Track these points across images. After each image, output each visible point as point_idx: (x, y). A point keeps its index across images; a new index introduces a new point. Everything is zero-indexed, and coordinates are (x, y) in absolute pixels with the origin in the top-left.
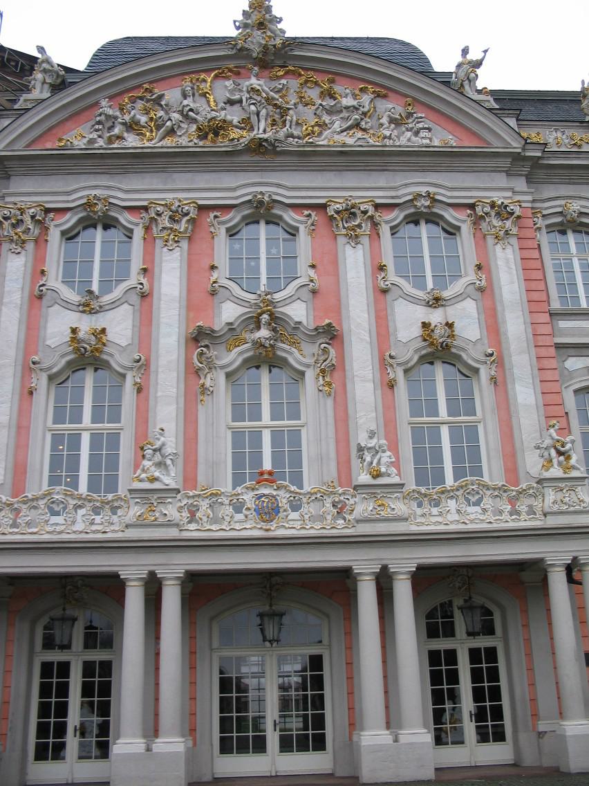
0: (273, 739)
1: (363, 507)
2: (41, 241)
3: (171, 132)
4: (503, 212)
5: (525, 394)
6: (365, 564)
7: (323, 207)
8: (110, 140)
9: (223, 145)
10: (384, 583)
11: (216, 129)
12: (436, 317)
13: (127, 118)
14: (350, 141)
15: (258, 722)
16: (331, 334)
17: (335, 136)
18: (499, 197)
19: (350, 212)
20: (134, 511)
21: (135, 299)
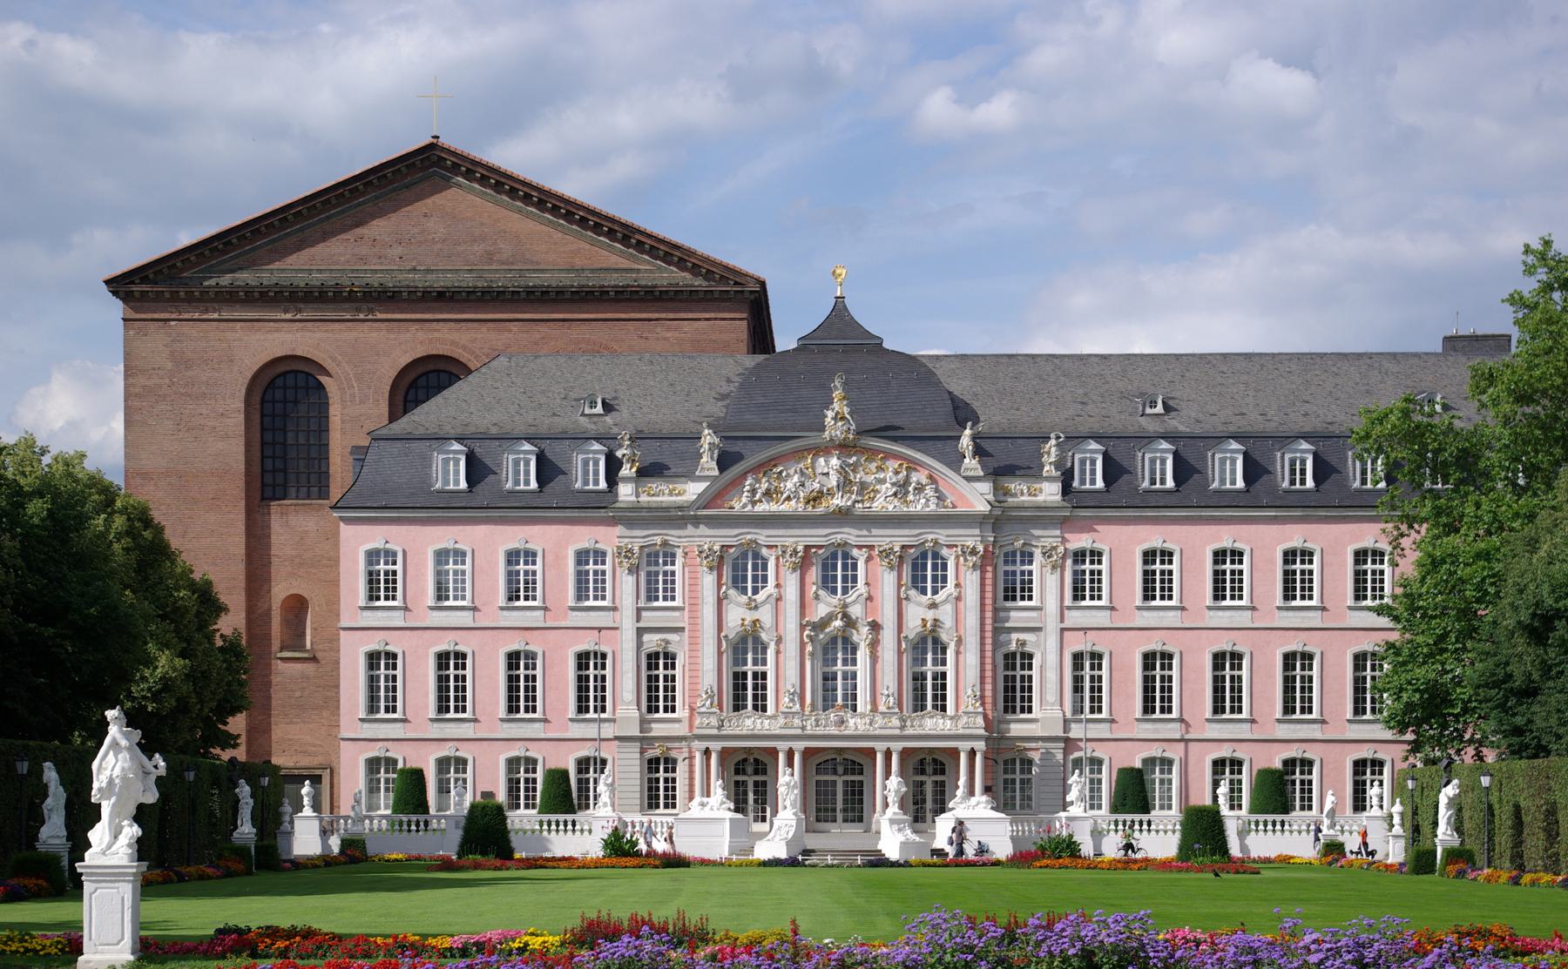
0: (840, 816)
1: (879, 720)
2: (719, 568)
3: (788, 499)
4: (974, 552)
5: (971, 658)
6: (880, 746)
7: (871, 547)
8: (754, 503)
9: (820, 510)
10: (888, 755)
11: (815, 498)
12: (930, 615)
13: (765, 486)
14: (891, 508)
15: (834, 810)
16: (875, 627)
17: (883, 503)
18: (970, 543)
19: (885, 554)
20: (782, 721)
21: (773, 600)
